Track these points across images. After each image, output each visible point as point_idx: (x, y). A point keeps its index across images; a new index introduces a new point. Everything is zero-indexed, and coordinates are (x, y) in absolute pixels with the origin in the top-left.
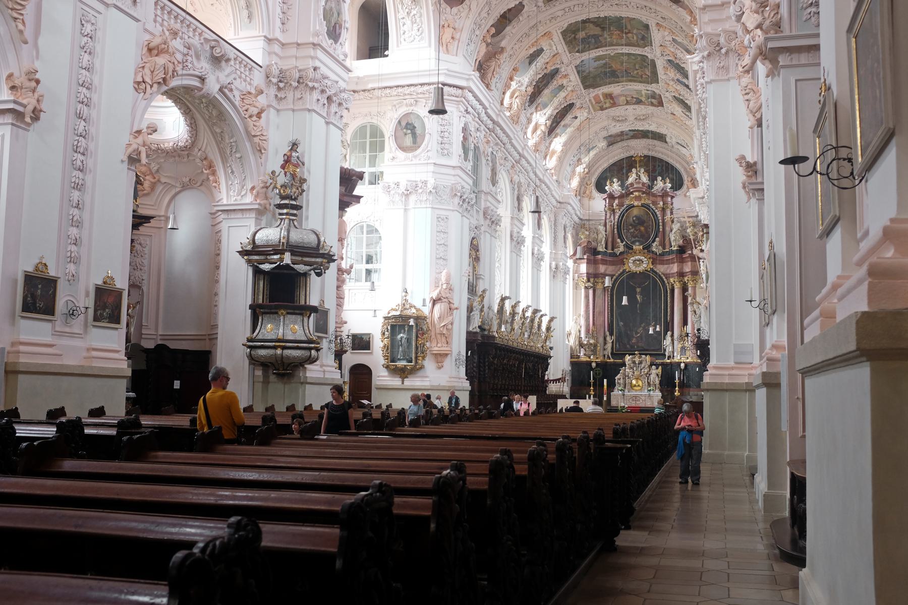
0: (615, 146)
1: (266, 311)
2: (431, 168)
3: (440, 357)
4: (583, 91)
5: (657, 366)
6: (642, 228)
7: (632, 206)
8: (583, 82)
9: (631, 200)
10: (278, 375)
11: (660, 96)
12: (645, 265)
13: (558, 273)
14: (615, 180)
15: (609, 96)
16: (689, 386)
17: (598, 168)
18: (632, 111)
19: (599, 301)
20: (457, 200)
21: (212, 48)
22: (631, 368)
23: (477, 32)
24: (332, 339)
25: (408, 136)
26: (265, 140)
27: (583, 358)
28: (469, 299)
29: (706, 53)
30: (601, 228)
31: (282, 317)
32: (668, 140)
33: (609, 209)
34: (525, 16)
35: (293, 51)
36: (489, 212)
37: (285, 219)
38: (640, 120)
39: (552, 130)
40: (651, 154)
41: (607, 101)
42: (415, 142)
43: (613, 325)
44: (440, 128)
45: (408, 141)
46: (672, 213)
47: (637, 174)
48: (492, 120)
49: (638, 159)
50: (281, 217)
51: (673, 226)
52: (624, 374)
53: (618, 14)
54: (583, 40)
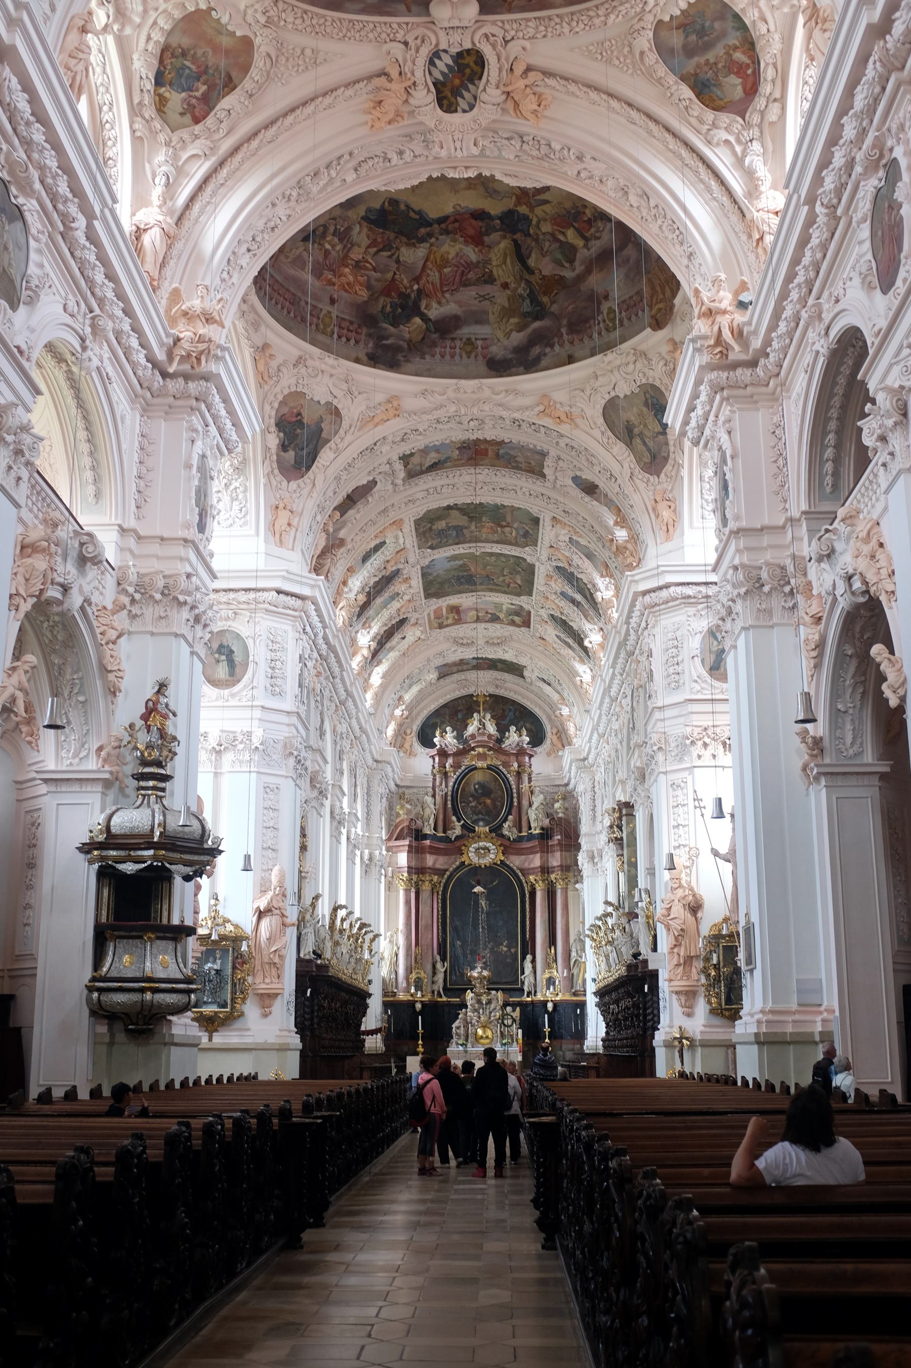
0: (449, 680)
1: (122, 933)
2: (258, 713)
3: (267, 999)
4: (424, 601)
5: (514, 1005)
6: (488, 801)
7: (476, 768)
8: (425, 590)
9: (472, 760)
10: (127, 1031)
11: (529, 613)
12: (492, 856)
13: (373, 867)
14: (448, 729)
15: (455, 610)
16: (561, 1037)
17: (421, 710)
19: (425, 909)
20: (291, 762)
21: (82, 544)
22: (475, 1010)
23: (319, 518)
27: (402, 996)
29: (743, 590)
30: (429, 799)
32: (526, 673)
33: (440, 771)
34: (376, 496)
35: (155, 548)
36: (320, 778)
37: (149, 796)
38: (493, 644)
39: (375, 655)
40: (501, 692)
41: (451, 615)
42: (232, 673)
43: (445, 947)
44: (270, 655)
45: (222, 671)
46: (530, 780)
47: (480, 721)
48: (327, 643)
49: (481, 700)
50: (143, 792)
51: (534, 799)
52: (465, 1020)
53: (499, 501)
54: (441, 533)
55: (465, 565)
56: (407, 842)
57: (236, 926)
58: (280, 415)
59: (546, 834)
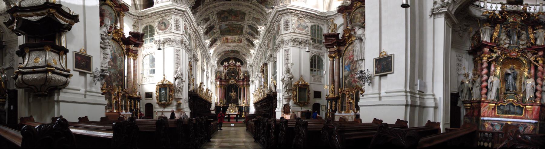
18: (232, 45)
28: (189, 81)
55: (228, 27)
56: (219, 80)
57: (169, 82)
59: (243, 79)
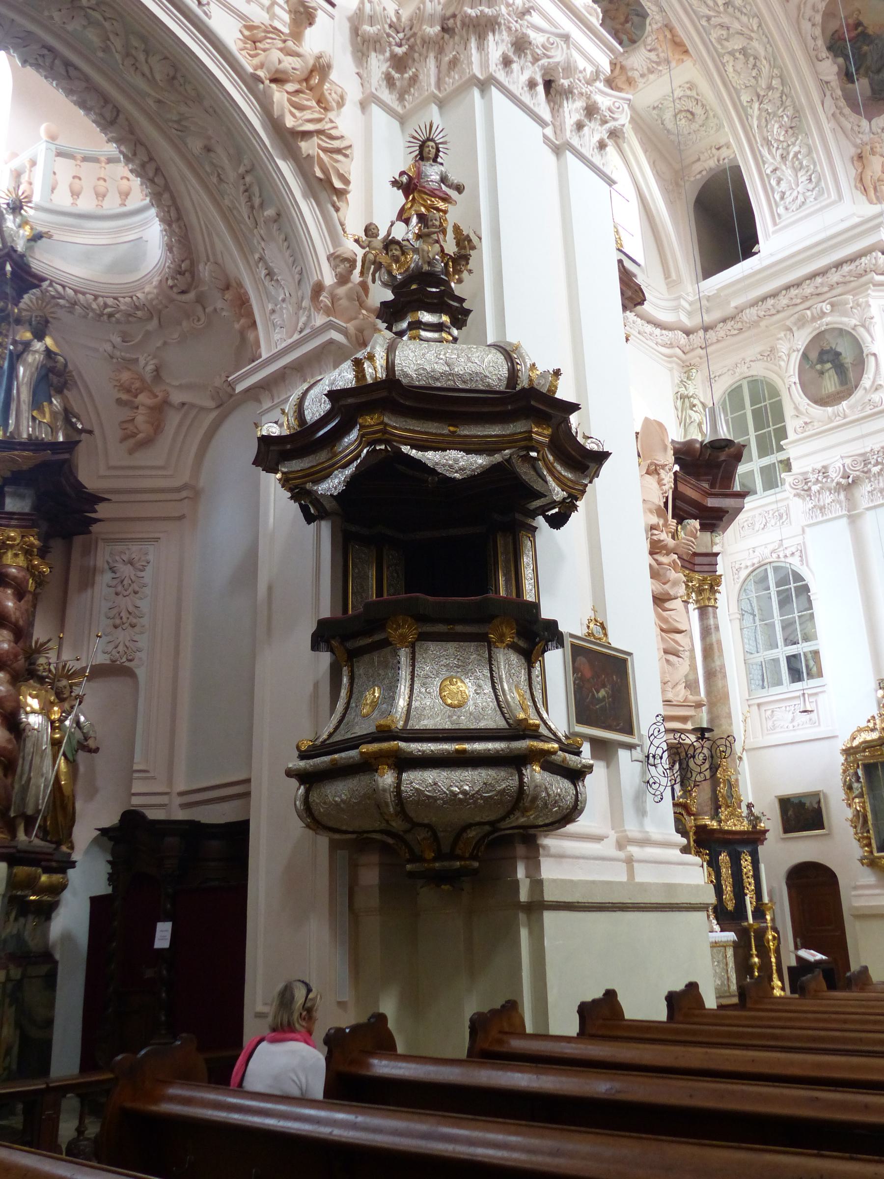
24: (652, 750)
25: (827, 374)
26: (338, 151)
31: (404, 655)
45: (830, 383)
58: (829, 33)
